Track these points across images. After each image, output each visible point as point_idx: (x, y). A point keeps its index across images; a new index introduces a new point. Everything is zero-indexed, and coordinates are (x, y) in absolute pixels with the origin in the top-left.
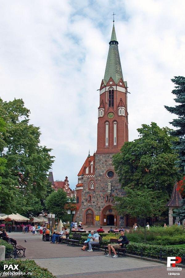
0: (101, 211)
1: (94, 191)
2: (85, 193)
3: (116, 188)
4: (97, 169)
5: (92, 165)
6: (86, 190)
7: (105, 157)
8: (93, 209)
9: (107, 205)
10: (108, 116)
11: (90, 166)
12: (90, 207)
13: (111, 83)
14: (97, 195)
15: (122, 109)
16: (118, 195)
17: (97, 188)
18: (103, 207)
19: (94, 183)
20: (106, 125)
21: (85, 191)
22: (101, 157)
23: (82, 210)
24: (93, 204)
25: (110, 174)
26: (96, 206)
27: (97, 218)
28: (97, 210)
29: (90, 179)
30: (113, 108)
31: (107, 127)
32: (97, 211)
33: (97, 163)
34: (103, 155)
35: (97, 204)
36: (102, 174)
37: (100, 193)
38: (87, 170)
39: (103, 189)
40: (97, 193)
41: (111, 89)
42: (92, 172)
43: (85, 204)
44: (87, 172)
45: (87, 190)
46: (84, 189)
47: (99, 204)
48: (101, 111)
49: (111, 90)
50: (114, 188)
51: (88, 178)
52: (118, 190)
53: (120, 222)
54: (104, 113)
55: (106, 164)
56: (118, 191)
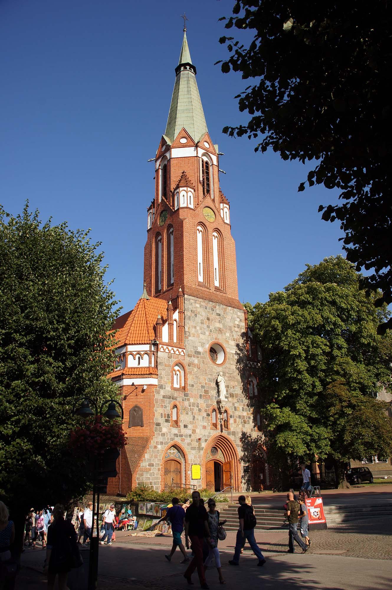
0: (202, 452)
2: (164, 397)
3: (231, 391)
4: (189, 336)
6: (166, 388)
12: (178, 440)
14: (194, 404)
16: (235, 409)
17: (193, 386)
18: (206, 440)
19: (178, 373)
21: (162, 392)
23: (155, 447)
24: (184, 431)
26: (190, 436)
28: (193, 448)
29: (174, 360)
32: (194, 452)
34: (202, 303)
35: (194, 431)
36: (200, 349)
39: (206, 392)
40: (192, 400)
41: (205, 159)
43: (164, 430)
44: (165, 338)
45: (168, 388)
47: (198, 431)
48: (190, 194)
55: (208, 327)
56: (235, 400)
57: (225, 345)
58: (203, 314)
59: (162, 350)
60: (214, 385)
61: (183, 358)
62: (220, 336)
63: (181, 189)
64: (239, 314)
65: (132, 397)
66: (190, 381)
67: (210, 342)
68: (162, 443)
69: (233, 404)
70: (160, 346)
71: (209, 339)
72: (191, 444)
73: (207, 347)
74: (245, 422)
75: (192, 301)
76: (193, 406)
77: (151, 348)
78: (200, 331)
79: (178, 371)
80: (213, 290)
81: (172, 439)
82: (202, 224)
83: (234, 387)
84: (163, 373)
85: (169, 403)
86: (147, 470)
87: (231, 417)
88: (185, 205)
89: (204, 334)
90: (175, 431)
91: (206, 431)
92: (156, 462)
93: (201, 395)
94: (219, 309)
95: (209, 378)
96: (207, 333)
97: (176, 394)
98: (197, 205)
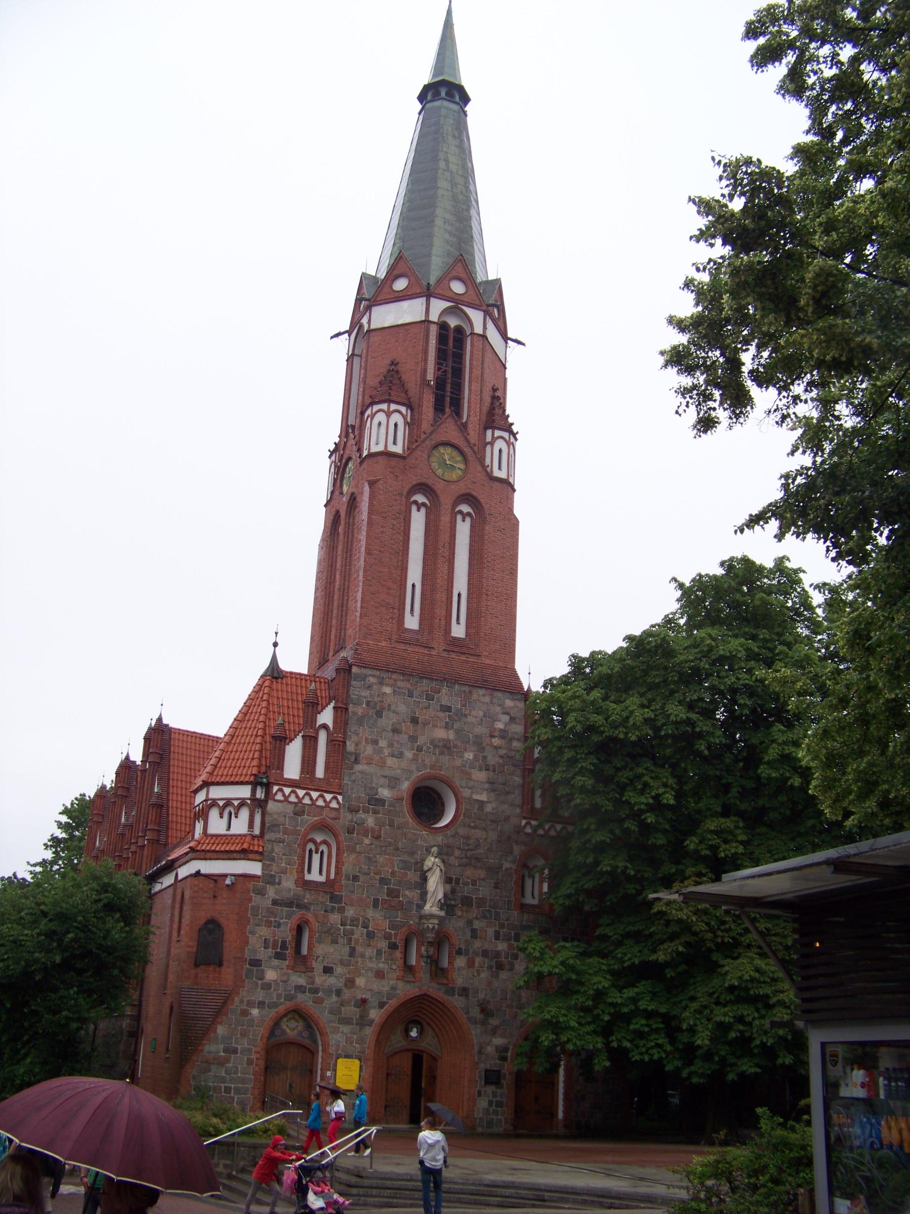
1: (334, 898)
2: (275, 902)
3: (466, 891)
4: (357, 761)
5: (324, 726)
7: (411, 695)
8: (323, 1015)
9: (406, 990)
10: (433, 459)
11: (311, 732)
12: (305, 1000)
13: (458, 288)
14: (354, 922)
15: (509, 444)
16: (474, 934)
17: (355, 878)
18: (382, 1005)
19: (323, 847)
20: (414, 508)
21: (271, 892)
22: (387, 690)
23: (245, 1013)
24: (320, 980)
25: (426, 801)
27: (348, 1073)
28: (347, 1021)
30: (465, 426)
31: (418, 520)
32: (346, 1029)
33: (360, 721)
34: (399, 684)
35: (350, 983)
36: (385, 793)
37: (371, 913)
38: (294, 752)
40: (350, 912)
41: (453, 322)
42: (320, 773)
43: (271, 975)
44: (292, 768)
45: (288, 883)
46: (269, 878)
47: (360, 982)
48: (396, 418)
49: (452, 326)
50: (453, 891)
51: (299, 810)
52: (478, 907)
53: (483, 1103)
54: (409, 434)
55: (413, 739)
57: (457, 782)
58: (402, 708)
59: (279, 797)
60: (413, 877)
61: (333, 814)
62: (445, 759)
63: (376, 408)
64: (509, 703)
65: (205, 901)
66: (347, 868)
67: (416, 774)
68: (261, 1005)
69: (470, 922)
70: (276, 788)
71: (413, 767)
72: (340, 1013)
73: (406, 786)
74: (500, 967)
75: (372, 680)
76: (354, 925)
77: (254, 792)
78: (386, 752)
79: (325, 842)
80: (439, 646)
81: (290, 998)
82: (424, 488)
83: (474, 883)
84: (278, 849)
85: (289, 917)
86: (221, 1063)
87: (459, 952)
88: (380, 448)
89: (400, 756)
90: (299, 980)
91: (385, 982)
92: (243, 1044)
93: (376, 901)
94: (446, 696)
95: (404, 862)
96: (409, 755)
97: (308, 898)
98: (413, 441)
